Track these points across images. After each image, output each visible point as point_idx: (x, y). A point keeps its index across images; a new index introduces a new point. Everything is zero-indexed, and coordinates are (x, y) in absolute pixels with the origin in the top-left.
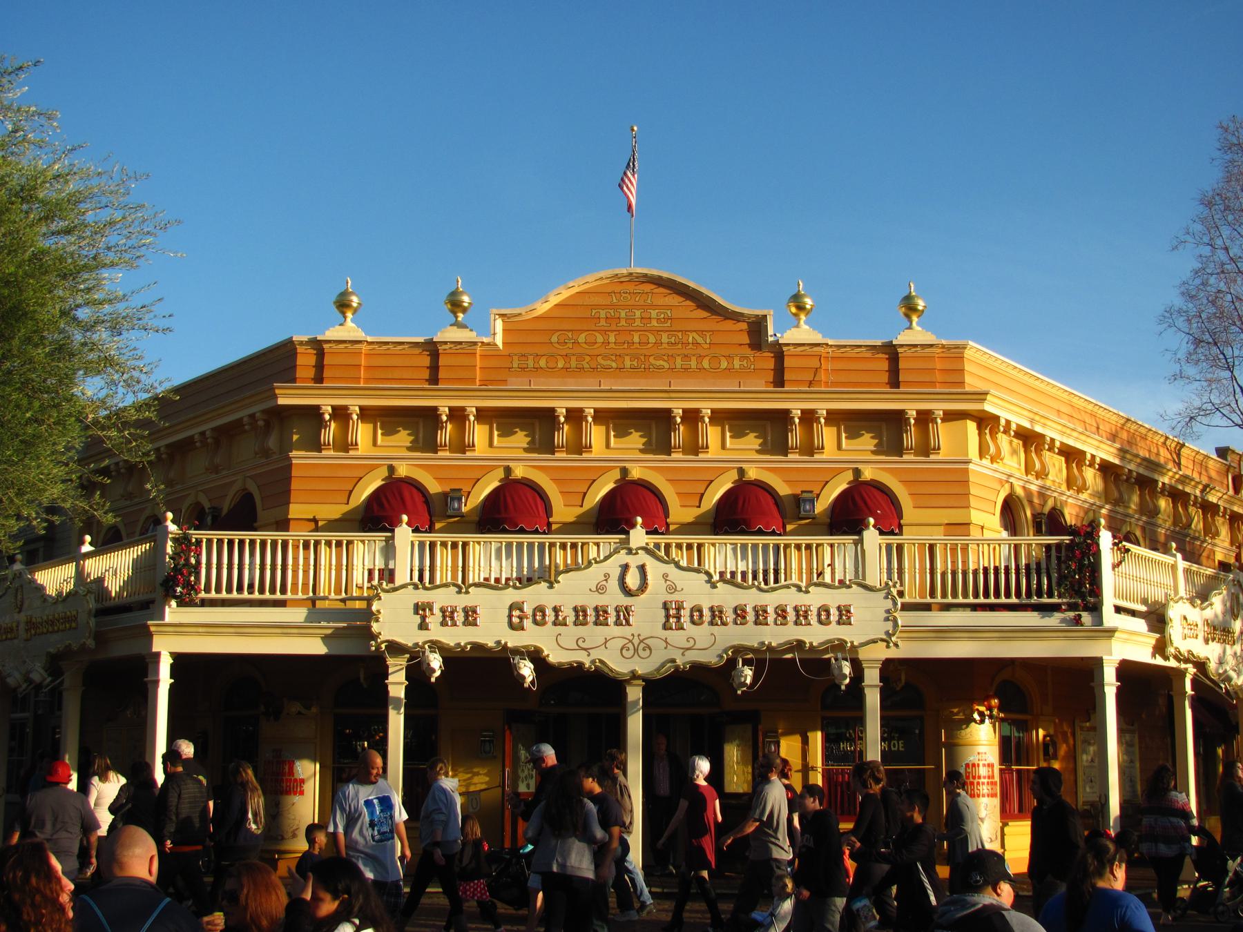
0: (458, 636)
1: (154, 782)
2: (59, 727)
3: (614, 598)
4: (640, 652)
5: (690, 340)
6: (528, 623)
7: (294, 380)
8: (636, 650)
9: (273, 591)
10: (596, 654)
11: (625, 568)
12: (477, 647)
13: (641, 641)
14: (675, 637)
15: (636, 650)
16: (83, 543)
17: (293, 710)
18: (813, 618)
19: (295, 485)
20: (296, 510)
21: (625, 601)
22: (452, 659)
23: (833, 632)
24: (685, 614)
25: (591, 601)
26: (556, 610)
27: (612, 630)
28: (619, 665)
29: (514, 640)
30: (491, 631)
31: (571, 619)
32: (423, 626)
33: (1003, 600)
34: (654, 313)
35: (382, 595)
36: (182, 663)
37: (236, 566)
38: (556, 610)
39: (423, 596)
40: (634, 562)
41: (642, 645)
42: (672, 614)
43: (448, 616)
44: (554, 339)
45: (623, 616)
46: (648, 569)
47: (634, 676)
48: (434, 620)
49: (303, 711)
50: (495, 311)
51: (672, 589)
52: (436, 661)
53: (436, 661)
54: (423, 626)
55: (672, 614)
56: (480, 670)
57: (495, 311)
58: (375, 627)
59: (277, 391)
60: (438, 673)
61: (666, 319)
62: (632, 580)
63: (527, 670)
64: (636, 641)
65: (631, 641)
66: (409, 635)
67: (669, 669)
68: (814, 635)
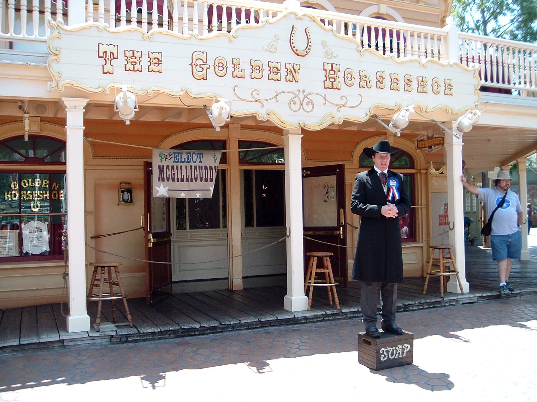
8: (302, 104)
10: (270, 106)
13: (305, 97)
15: (302, 104)
21: (293, 59)
25: (264, 59)
26: (236, 66)
27: (283, 85)
31: (249, 71)
41: (306, 100)
45: (293, 73)
51: (328, 54)
58: (55, 68)
62: (300, 44)
64: (301, 96)
65: (297, 96)
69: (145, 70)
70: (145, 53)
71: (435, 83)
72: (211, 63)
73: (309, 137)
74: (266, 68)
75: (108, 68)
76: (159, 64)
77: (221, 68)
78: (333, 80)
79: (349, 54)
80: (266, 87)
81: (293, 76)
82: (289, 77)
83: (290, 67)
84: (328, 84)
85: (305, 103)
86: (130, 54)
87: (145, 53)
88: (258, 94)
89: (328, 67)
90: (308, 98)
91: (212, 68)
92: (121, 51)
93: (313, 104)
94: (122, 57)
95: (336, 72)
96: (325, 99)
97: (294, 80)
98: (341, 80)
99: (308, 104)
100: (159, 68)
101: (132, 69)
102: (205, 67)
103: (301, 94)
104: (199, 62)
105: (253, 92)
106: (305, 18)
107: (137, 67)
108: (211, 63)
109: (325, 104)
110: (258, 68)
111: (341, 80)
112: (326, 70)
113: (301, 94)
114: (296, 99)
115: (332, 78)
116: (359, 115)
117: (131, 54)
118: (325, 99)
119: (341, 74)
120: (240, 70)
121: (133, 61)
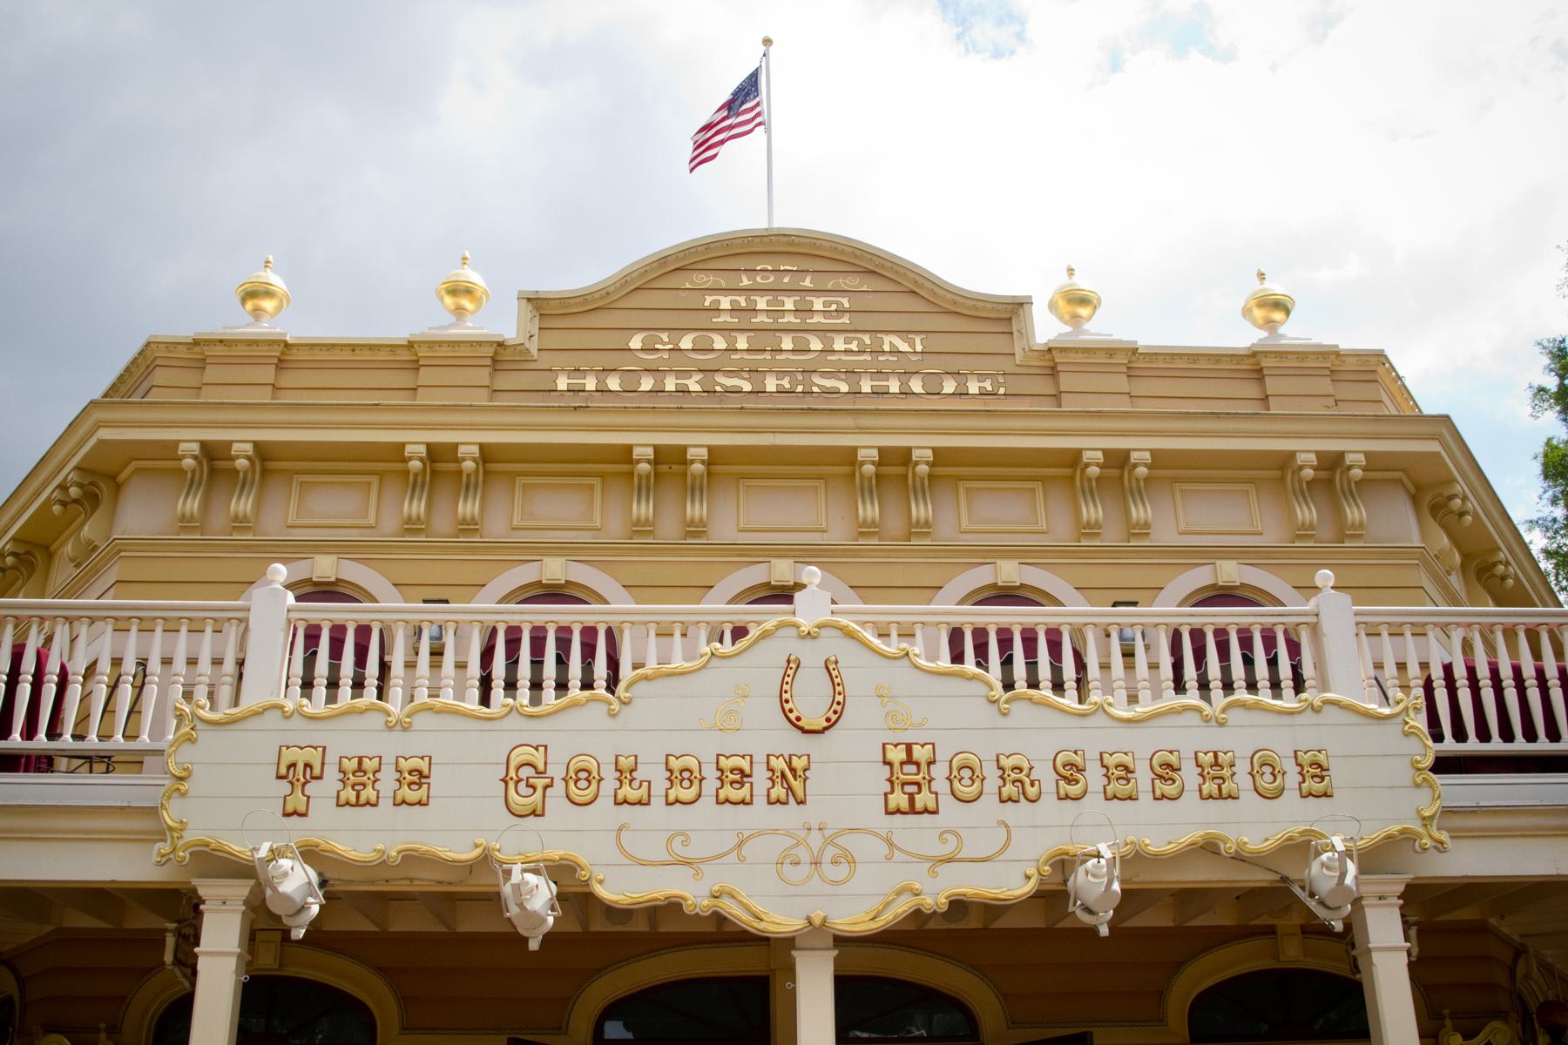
3: (767, 739)
4: (828, 870)
11: (792, 666)
13: (830, 841)
14: (915, 833)
23: (1286, 818)
26: (625, 774)
28: (773, 910)
34: (818, 304)
41: (830, 852)
43: (358, 775)
45: (790, 782)
46: (848, 675)
47: (816, 931)
61: (841, 311)
64: (816, 840)
67: (903, 906)
68: (1254, 826)
69: (386, 803)
70: (389, 759)
72: (556, 771)
74: (711, 773)
75: (297, 801)
76: (420, 785)
77: (583, 784)
78: (914, 789)
79: (964, 715)
80: (708, 824)
81: (790, 788)
82: (779, 791)
85: (827, 857)
87: (389, 759)
88: (685, 844)
89: (897, 755)
90: (837, 846)
91: (559, 786)
92: (332, 758)
93: (852, 862)
94: (332, 773)
95: (924, 767)
96: (891, 844)
97: (791, 799)
98: (941, 785)
99: (835, 862)
100: (421, 793)
101: (353, 800)
103: (815, 834)
104: (526, 772)
105: (670, 840)
106: (824, 632)
107: (368, 793)
108: (556, 771)
109: (888, 858)
110: (686, 774)
111: (941, 785)
112: (890, 764)
113: (815, 834)
114: (802, 854)
115: (910, 782)
116: (1009, 882)
118: (891, 844)
119: (939, 771)
120: (636, 784)
121: (358, 783)
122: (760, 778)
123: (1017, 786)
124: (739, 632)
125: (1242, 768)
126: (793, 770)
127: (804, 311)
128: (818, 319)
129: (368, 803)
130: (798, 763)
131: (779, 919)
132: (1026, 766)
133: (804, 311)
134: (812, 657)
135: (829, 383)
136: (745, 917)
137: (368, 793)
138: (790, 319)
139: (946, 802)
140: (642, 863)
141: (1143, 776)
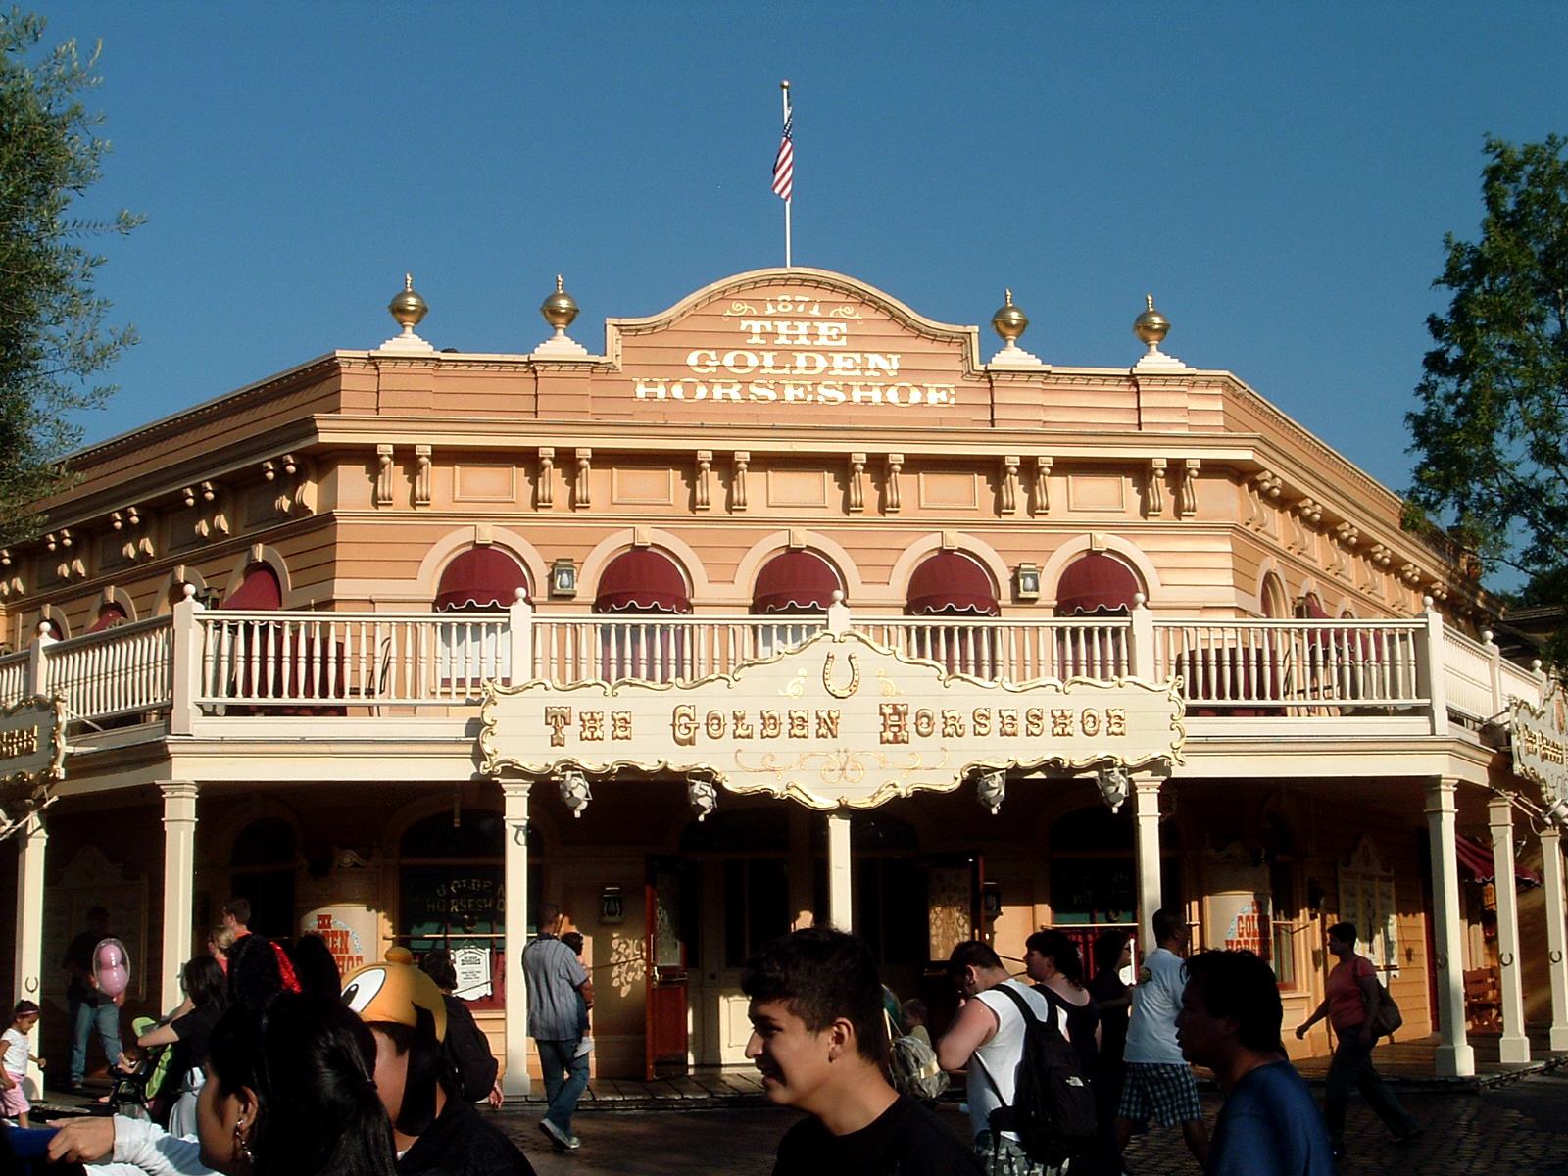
0: (602, 757)
1: (693, 1053)
2: (503, 948)
5: (872, 366)
6: (701, 736)
7: (338, 410)
9: (263, 693)
12: (629, 770)
16: (39, 632)
17: (347, 860)
18: (1075, 727)
19: (341, 552)
20: (341, 588)
22: (598, 783)
24: (910, 719)
29: (678, 760)
30: (651, 751)
31: (758, 727)
32: (557, 742)
33: (1255, 701)
34: (823, 328)
35: (498, 697)
36: (214, 799)
37: (271, 659)
38: (738, 719)
39: (558, 700)
40: (840, 652)
42: (895, 724)
43: (591, 722)
44: (692, 358)
45: (828, 726)
48: (572, 732)
49: (361, 862)
50: (616, 321)
52: (579, 791)
53: (579, 791)
54: (557, 742)
55: (895, 724)
56: (641, 803)
57: (610, 321)
59: (318, 424)
60: (584, 805)
61: (840, 336)
63: (704, 797)
66: (538, 757)
67: (888, 795)
71: (1088, 717)
73: (861, 820)
77: (716, 727)
78: (896, 729)
82: (823, 731)
83: (824, 715)
84: (889, 735)
85: (848, 767)
86: (587, 717)
89: (888, 710)
94: (576, 721)
97: (829, 736)
101: (590, 737)
102: (692, 727)
104: (685, 720)
105: (764, 758)
107: (598, 733)
113: (842, 754)
117: (589, 716)
122: (813, 723)
123: (953, 729)
124: (797, 629)
125: (1077, 718)
126: (830, 718)
127: (813, 335)
128: (823, 341)
129: (598, 738)
130: (833, 715)
131: (822, 801)
132: (958, 717)
133: (813, 335)
134: (840, 652)
135: (832, 393)
136: (805, 799)
137: (598, 733)
138: (803, 341)
139: (914, 736)
140: (746, 768)
141: (1022, 723)
